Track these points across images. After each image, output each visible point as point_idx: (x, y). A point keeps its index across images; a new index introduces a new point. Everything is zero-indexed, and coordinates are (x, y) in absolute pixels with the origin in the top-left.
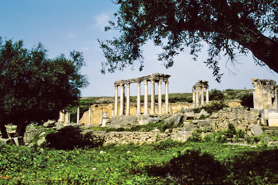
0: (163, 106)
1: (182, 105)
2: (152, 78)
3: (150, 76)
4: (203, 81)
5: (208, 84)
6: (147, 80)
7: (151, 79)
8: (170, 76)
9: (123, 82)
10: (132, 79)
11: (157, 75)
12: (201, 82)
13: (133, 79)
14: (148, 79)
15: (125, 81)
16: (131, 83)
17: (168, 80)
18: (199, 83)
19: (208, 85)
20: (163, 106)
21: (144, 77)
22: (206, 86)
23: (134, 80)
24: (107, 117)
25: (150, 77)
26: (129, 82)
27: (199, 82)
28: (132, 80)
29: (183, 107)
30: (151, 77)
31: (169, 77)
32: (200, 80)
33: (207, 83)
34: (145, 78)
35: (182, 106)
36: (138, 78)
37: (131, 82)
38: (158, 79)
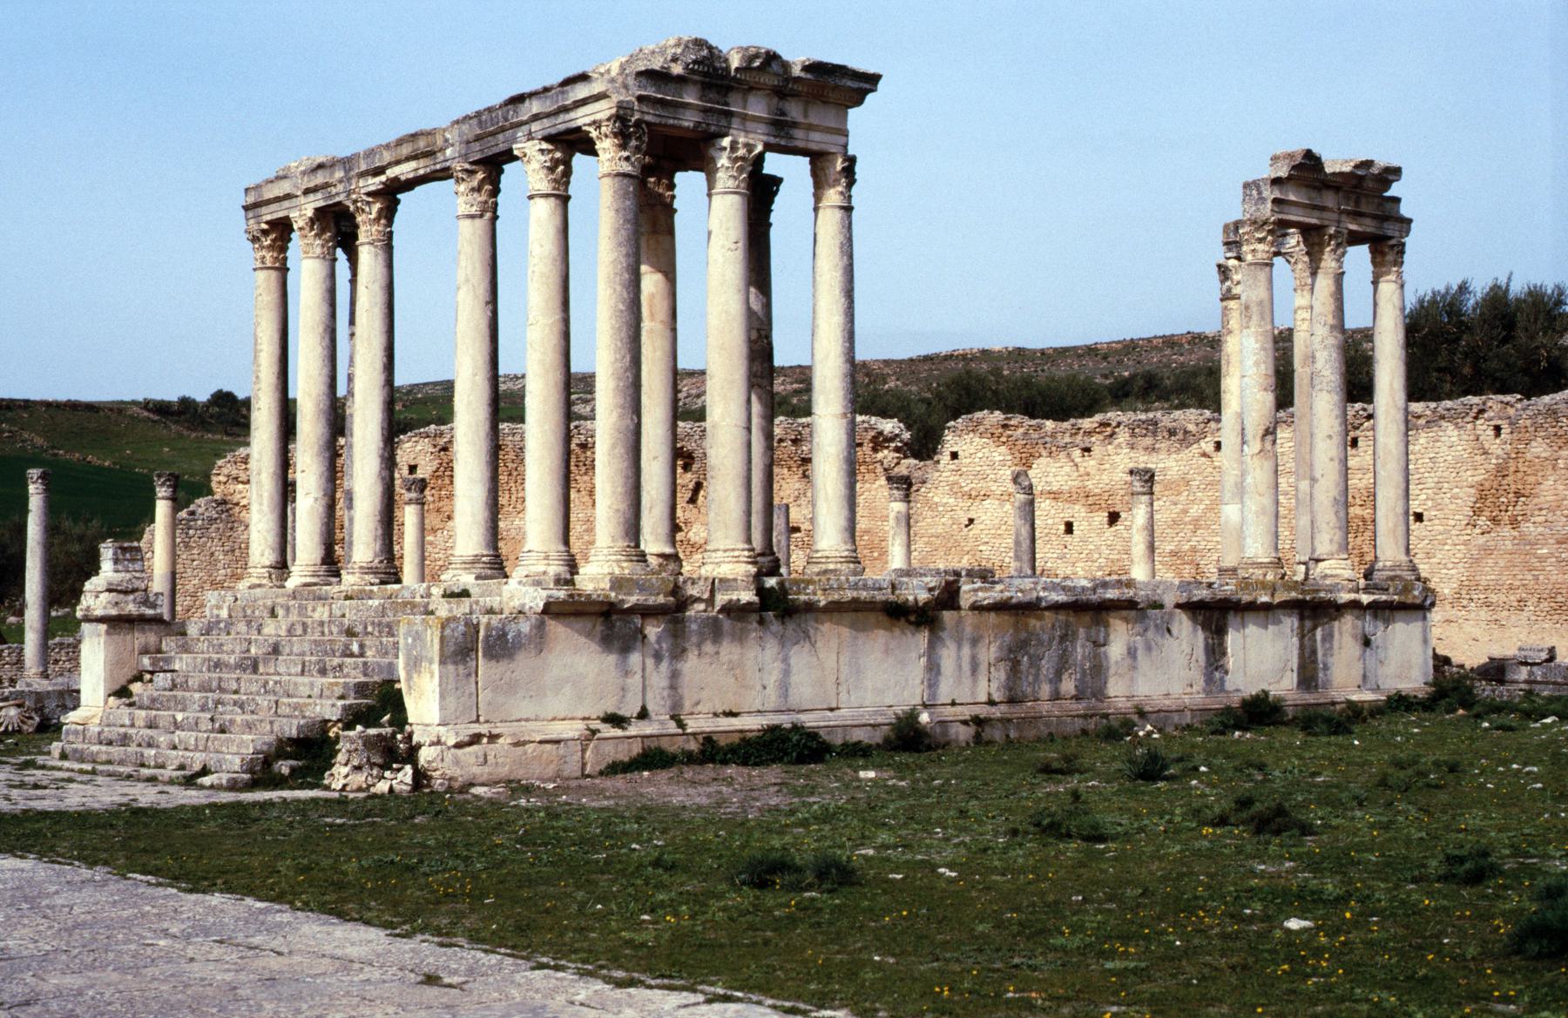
0: (954, 456)
1: (1148, 441)
2: (603, 110)
3: (583, 78)
4: (1337, 160)
5: (1397, 200)
6: (547, 139)
7: (597, 124)
8: (872, 80)
9: (319, 179)
10: (400, 142)
11: (677, 69)
12: (1307, 168)
13: (414, 137)
14: (561, 123)
15: (339, 174)
16: (410, 185)
17: (845, 134)
18: (1276, 182)
19: (1405, 210)
20: (954, 456)
21: (518, 100)
22: (1368, 226)
23: (422, 144)
24: (131, 608)
25: (581, 91)
26: (375, 183)
27: (1283, 172)
28: (406, 150)
29: (1143, 460)
30: (596, 88)
31: (858, 98)
32: (1297, 146)
33: (1393, 191)
34: (535, 107)
35: (1152, 449)
36: (459, 115)
37: (391, 173)
38: (689, 120)
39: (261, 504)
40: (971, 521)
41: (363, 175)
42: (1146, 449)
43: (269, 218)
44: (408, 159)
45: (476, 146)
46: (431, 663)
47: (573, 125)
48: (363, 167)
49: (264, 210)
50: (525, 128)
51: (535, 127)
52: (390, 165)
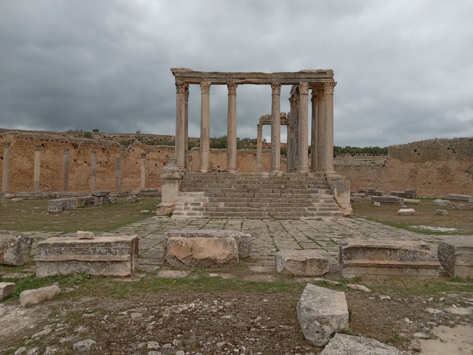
1: (171, 151)
20: (133, 150)
30: (327, 76)
39: (182, 151)
40: (137, 163)
41: (235, 78)
42: (171, 152)
43: (185, 81)
44: (256, 78)
45: (284, 80)
46: (347, 190)
47: (320, 82)
48: (234, 76)
49: (185, 79)
50: (304, 80)
51: (306, 80)
52: (247, 78)
